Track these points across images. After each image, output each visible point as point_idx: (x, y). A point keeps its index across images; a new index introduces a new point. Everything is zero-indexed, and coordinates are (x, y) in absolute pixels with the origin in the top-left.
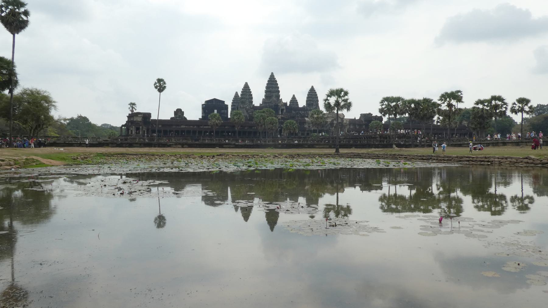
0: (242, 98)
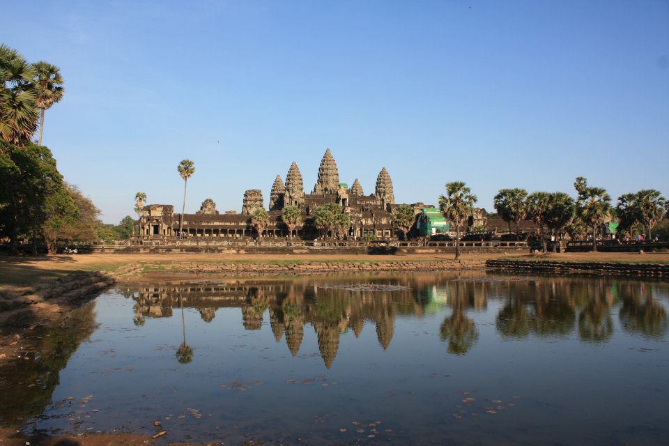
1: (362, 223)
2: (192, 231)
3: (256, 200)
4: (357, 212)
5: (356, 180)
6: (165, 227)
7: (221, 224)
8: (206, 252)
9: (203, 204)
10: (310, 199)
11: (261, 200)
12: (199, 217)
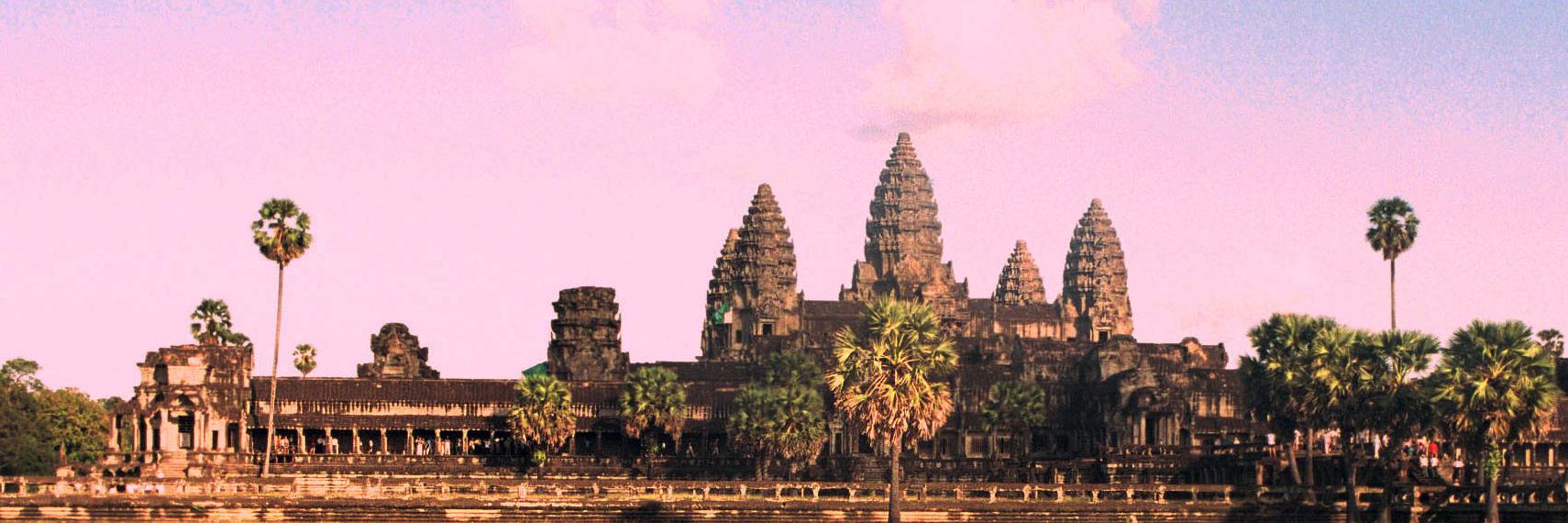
5: (1018, 245)
6: (220, 425)
7: (414, 411)
11: (615, 326)
12: (366, 385)
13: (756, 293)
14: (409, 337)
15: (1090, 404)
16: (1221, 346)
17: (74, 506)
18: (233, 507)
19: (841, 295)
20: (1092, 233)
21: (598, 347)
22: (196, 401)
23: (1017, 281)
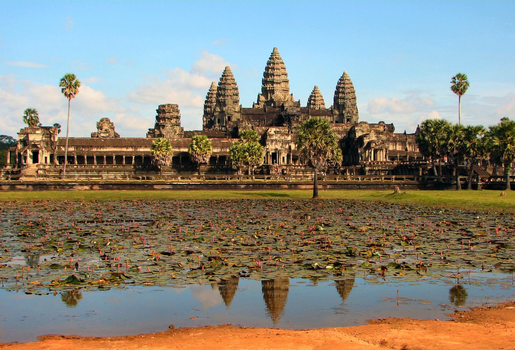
0: (218, 95)
1: (290, 147)
2: (81, 159)
3: (170, 119)
4: (282, 134)
6: (48, 155)
8: (55, 188)
9: (98, 124)
10: (247, 113)
11: (178, 118)
12: (94, 141)
13: (225, 106)
14: (110, 123)
15: (352, 146)
16: (392, 124)
17: (28, 185)
18: (83, 185)
19: (253, 106)
20: (344, 84)
21: (173, 125)
22: (39, 146)
23: (314, 100)
